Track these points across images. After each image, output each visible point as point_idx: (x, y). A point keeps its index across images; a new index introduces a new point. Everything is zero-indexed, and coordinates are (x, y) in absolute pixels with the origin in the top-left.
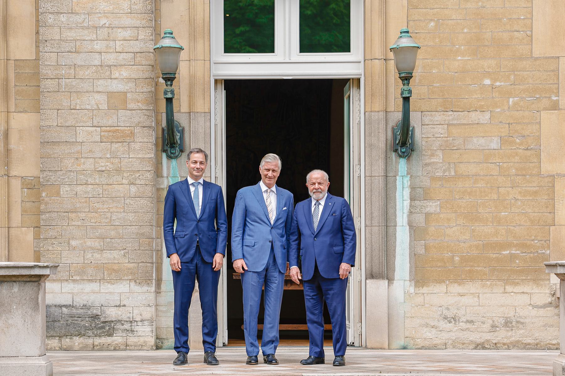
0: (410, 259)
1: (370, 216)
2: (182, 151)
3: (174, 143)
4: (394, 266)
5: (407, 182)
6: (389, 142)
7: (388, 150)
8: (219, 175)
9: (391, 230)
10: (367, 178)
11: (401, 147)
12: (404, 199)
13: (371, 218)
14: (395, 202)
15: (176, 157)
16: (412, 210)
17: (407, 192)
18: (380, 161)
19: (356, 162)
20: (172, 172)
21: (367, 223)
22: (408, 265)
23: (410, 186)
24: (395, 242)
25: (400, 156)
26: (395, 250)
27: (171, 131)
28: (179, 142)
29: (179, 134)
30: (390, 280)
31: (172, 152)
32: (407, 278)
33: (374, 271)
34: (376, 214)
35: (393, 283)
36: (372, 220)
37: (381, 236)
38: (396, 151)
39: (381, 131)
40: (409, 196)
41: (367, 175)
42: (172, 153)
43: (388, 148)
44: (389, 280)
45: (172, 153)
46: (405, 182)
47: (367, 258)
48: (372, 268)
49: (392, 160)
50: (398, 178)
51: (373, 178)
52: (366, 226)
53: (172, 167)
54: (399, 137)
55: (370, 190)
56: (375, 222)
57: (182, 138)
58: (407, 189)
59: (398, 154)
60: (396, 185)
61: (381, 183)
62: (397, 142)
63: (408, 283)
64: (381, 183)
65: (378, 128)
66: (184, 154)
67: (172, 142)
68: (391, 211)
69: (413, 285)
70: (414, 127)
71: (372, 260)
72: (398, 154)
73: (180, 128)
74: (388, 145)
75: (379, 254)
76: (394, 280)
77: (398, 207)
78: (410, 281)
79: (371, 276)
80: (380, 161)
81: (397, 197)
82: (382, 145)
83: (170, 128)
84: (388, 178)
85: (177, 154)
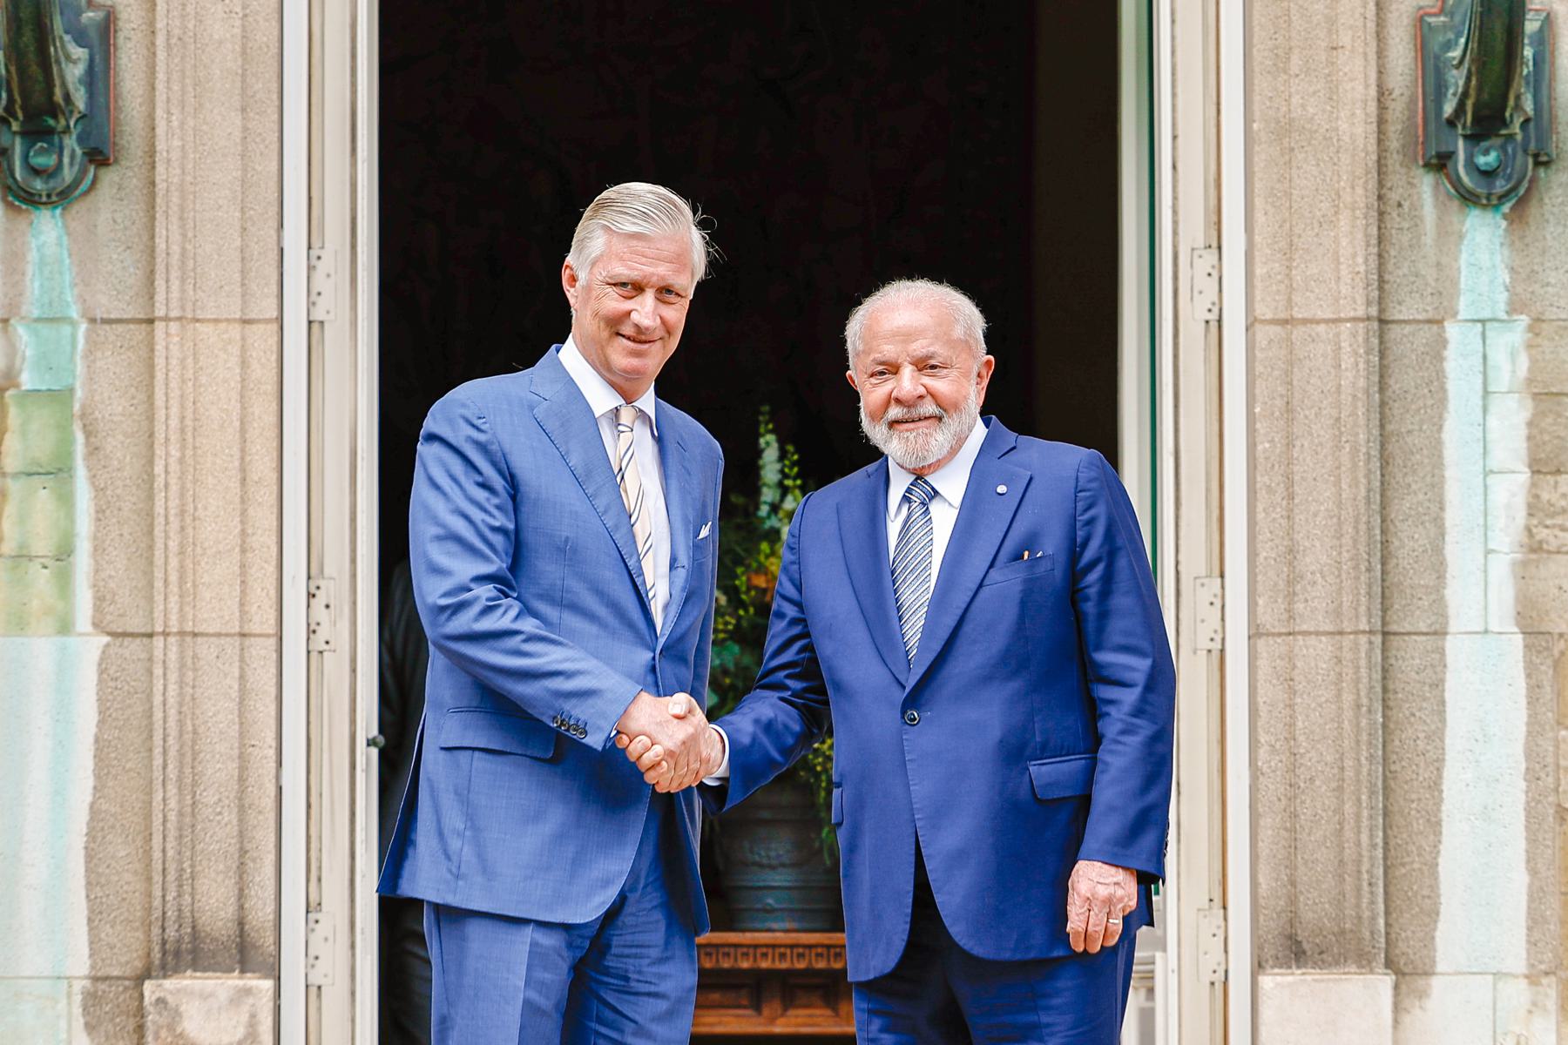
0: (1532, 840)
1: (1278, 573)
2: (98, 157)
3: (54, 111)
4: (1434, 888)
5: (1513, 356)
6: (1397, 109)
7: (1394, 160)
8: (331, 307)
9: (1410, 656)
10: (1263, 333)
11: (1474, 138)
12: (1493, 464)
13: (1290, 583)
14: (1436, 486)
15: (63, 197)
16: (1542, 533)
17: (1510, 421)
18: (1344, 222)
19: (1195, 230)
20: (33, 287)
21: (1266, 618)
22: (1521, 879)
23: (1530, 381)
24: (1437, 736)
25: (1468, 198)
26: (1435, 785)
27: (28, 37)
28: (80, 100)
29: (79, 53)
30: (1406, 969)
31: (39, 161)
32: (1516, 958)
33: (1307, 915)
34: (1316, 556)
35: (1422, 994)
36: (1291, 596)
37: (1348, 698)
38: (1440, 163)
39: (1345, 39)
40: (1521, 446)
41: (1263, 311)
42: (37, 172)
43: (1394, 143)
44: (1399, 973)
45: (37, 172)
46: (1498, 357)
47: (1266, 834)
48: (1293, 900)
49: (1416, 221)
50: (1452, 330)
51: (1299, 333)
52: (1255, 633)
53: (33, 256)
54: (1457, 79)
55: (1279, 411)
56: (1315, 609)
57: (100, 76)
58: (1512, 402)
59: (1457, 183)
60: (1440, 375)
61: (1347, 361)
62: (1449, 109)
63: (1517, 993)
64: (1347, 361)
65: (1331, 21)
66: (109, 176)
67: (38, 98)
68: (1409, 541)
69: (1552, 1004)
70: (1548, 21)
71: (1293, 845)
72: (1457, 183)
73: (89, 16)
74: (1394, 129)
75: (1339, 810)
76: (1429, 973)
77: (1459, 511)
78: (1532, 978)
79: (1290, 946)
80: (1344, 222)
81: (1450, 453)
82: (1354, 126)
83: (25, 14)
84: (1395, 332)
85: (68, 174)
